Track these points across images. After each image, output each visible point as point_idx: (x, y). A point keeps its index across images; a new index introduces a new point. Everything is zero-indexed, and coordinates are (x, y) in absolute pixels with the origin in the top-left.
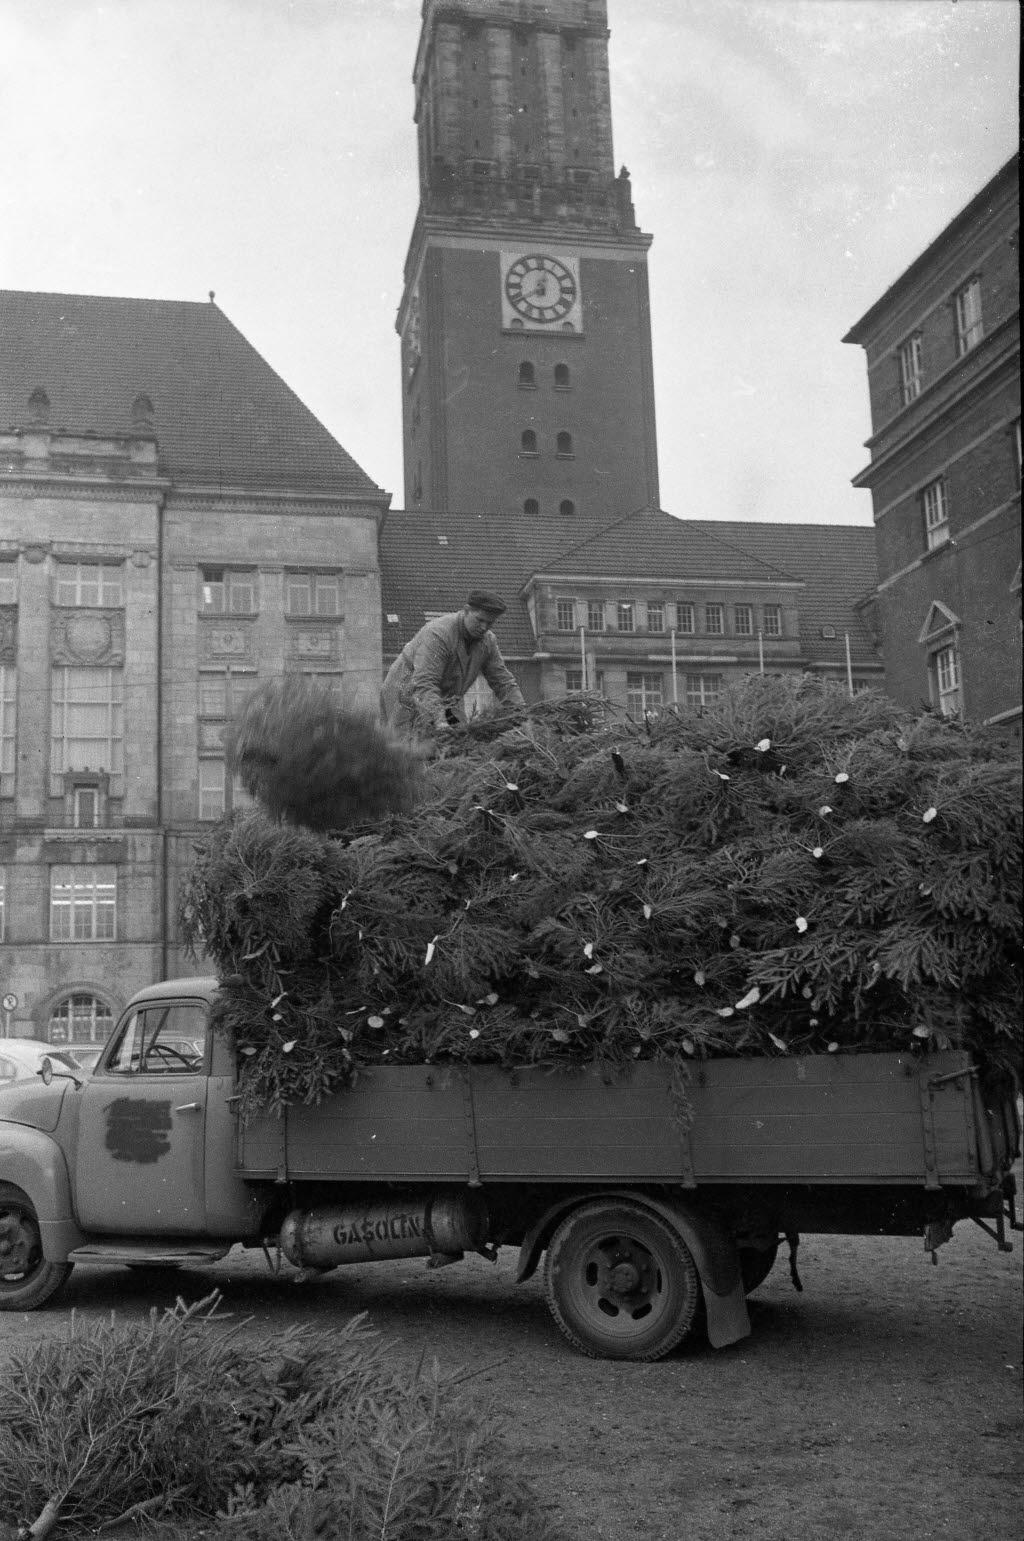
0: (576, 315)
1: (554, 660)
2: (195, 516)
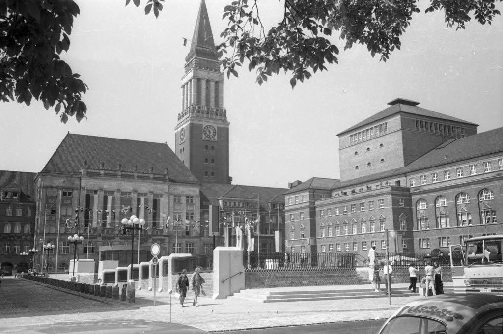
0: (216, 137)
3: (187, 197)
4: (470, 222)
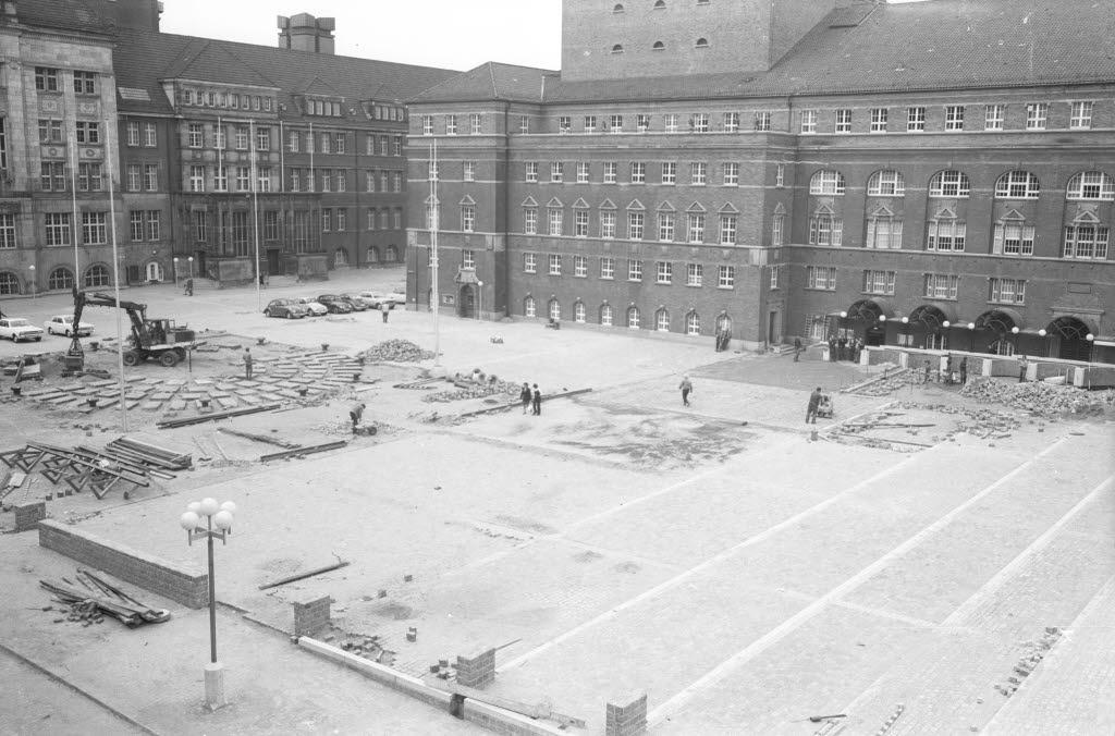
2: (32, 42)
3: (77, 73)
4: (959, 243)
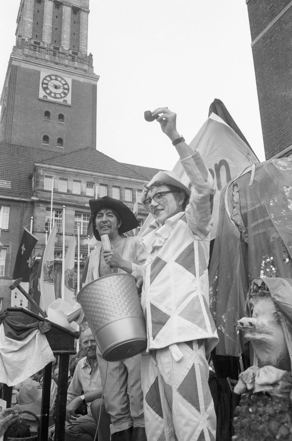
0: (69, 99)
1: (40, 202)
